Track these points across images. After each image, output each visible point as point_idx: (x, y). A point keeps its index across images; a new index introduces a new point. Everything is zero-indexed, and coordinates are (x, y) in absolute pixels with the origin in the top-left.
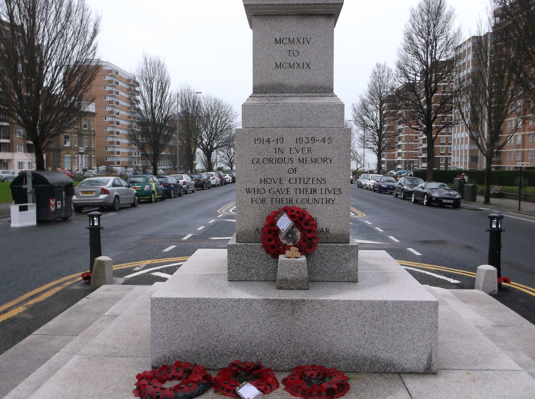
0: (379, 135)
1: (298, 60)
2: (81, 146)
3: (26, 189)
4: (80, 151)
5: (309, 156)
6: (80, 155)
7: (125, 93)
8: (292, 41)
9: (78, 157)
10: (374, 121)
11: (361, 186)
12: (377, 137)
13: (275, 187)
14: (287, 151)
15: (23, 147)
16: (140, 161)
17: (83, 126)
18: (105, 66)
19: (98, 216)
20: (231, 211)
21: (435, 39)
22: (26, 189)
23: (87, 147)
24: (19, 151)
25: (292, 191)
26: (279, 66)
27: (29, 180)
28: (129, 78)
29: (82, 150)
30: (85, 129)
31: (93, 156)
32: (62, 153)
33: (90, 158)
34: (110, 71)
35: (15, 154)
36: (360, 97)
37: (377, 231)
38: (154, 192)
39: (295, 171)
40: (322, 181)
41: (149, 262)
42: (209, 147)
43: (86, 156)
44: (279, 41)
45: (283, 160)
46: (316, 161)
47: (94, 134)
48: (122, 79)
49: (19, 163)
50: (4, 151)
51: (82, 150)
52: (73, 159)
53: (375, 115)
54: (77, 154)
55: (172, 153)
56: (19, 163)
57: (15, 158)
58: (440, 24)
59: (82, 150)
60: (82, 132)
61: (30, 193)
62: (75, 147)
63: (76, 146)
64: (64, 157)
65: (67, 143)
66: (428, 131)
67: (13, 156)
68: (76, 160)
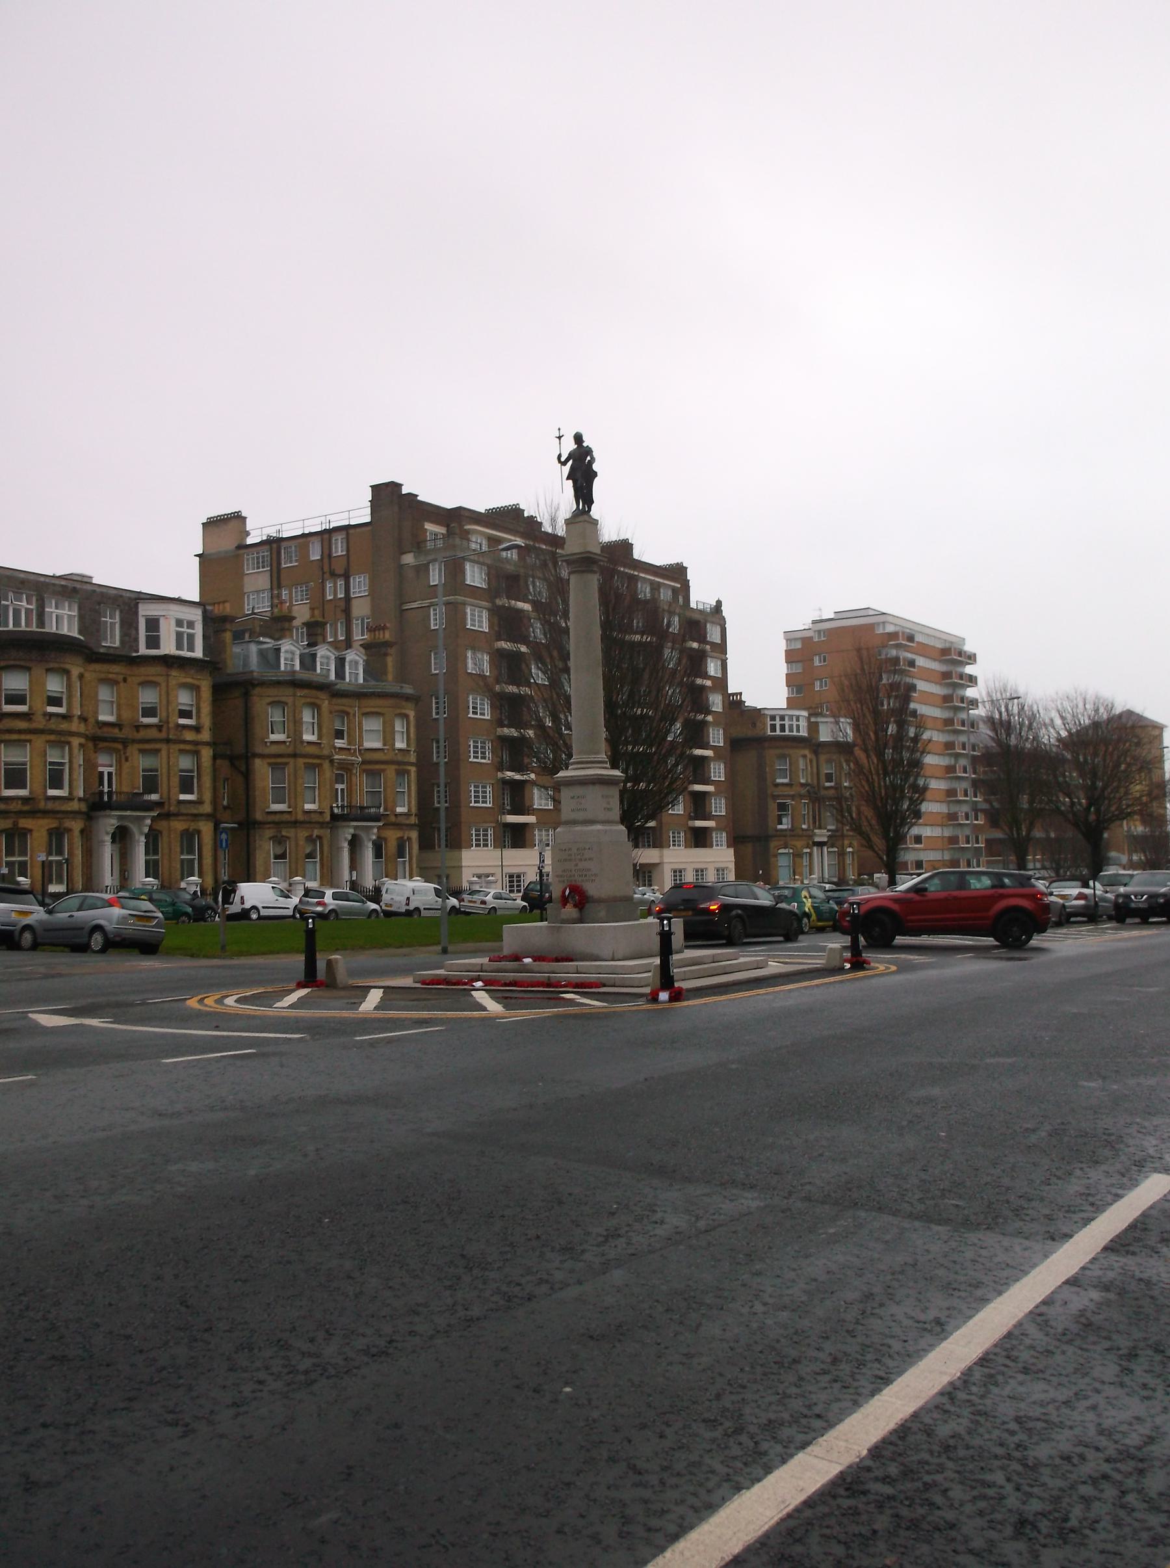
2: (820, 828)
4: (817, 839)
6: (815, 848)
7: (936, 683)
9: (811, 854)
15: (682, 834)
16: (983, 859)
17: (823, 778)
18: (878, 624)
23: (833, 827)
24: (674, 845)
28: (947, 645)
29: (821, 835)
30: (827, 784)
31: (850, 850)
32: (773, 844)
33: (842, 854)
34: (894, 636)
35: (666, 851)
38: (808, 915)
40: (589, 870)
42: (1092, 817)
43: (830, 850)
44: (573, 798)
47: (851, 794)
48: (925, 650)
49: (675, 871)
50: (644, 846)
51: (821, 835)
52: (797, 860)
54: (807, 847)
55: (1047, 832)
56: (675, 871)
57: (665, 861)
59: (821, 836)
60: (823, 792)
62: (803, 830)
63: (804, 827)
64: (776, 856)
65: (784, 820)
67: (661, 857)
68: (805, 861)
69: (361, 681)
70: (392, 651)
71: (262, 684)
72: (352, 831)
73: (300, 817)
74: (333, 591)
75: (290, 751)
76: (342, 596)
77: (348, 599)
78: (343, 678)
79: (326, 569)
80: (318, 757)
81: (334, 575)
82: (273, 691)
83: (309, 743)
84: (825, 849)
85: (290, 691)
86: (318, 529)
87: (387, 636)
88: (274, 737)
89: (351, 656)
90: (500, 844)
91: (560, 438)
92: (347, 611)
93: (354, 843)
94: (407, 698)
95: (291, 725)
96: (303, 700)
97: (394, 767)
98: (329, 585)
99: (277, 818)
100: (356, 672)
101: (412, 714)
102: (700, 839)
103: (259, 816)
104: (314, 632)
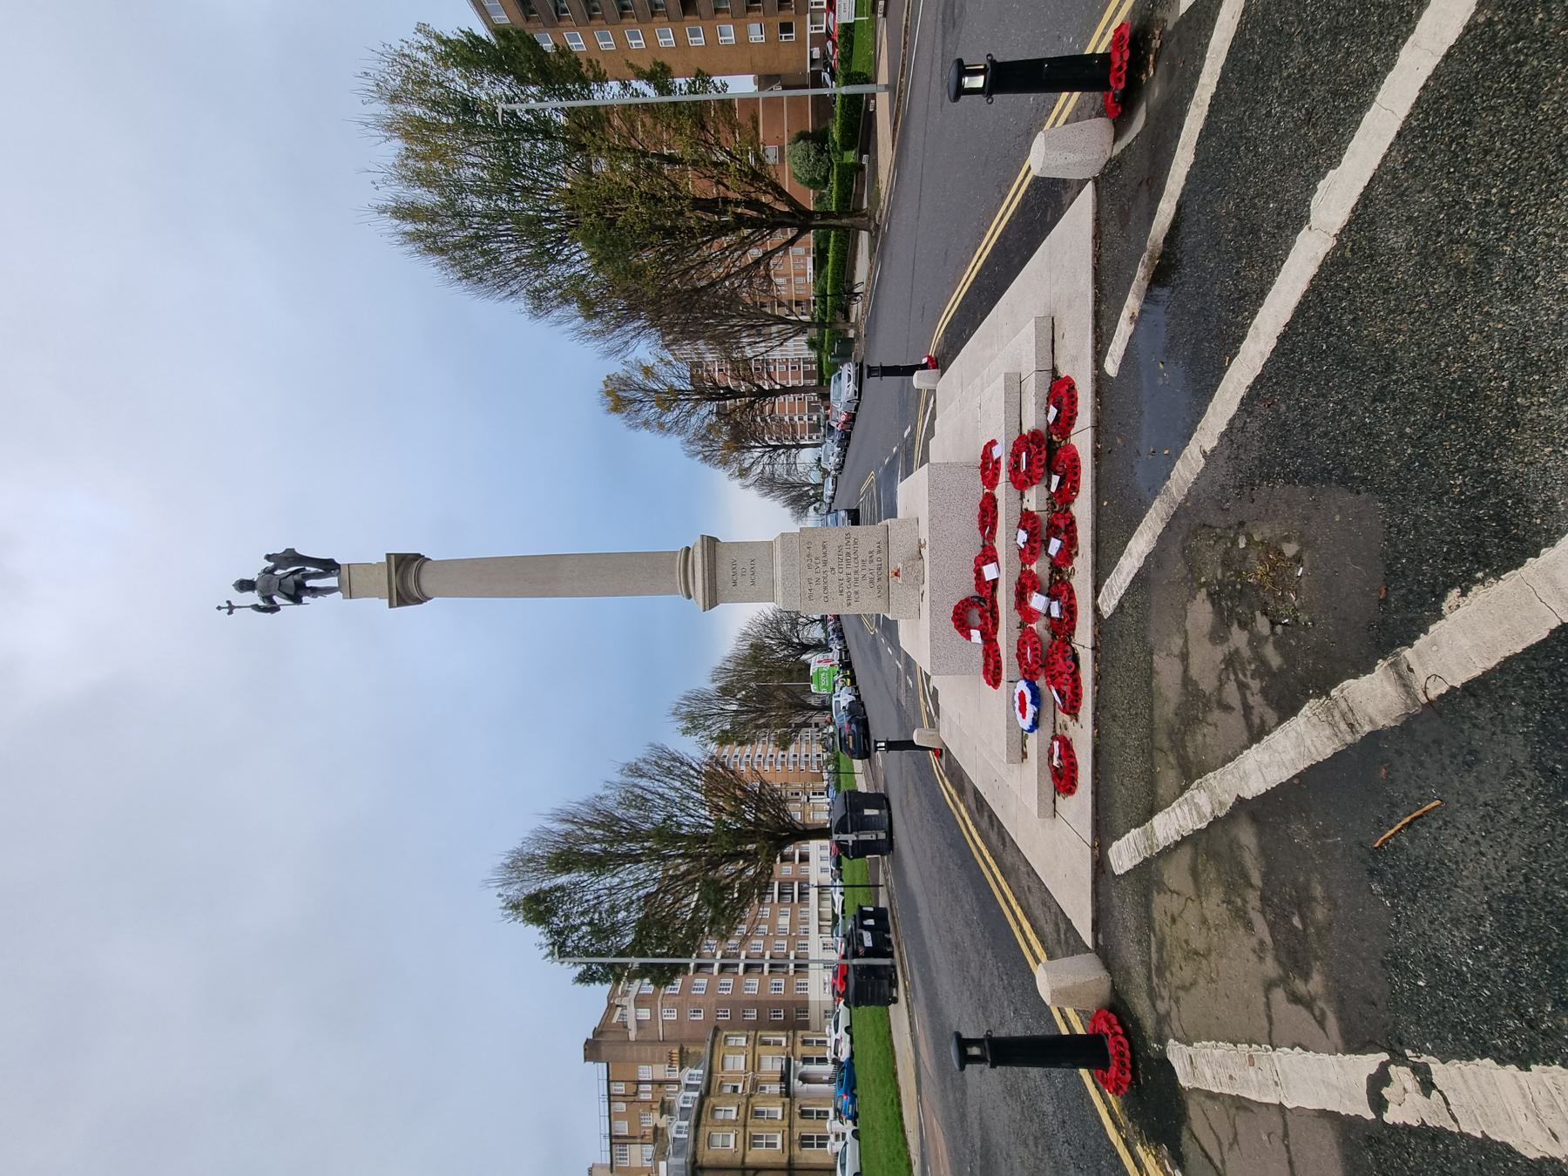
1: (748, 568)
3: (853, 841)
5: (821, 559)
8: (735, 574)
11: (840, 467)
13: (845, 584)
14: (817, 575)
19: (876, 742)
22: (853, 841)
25: (849, 571)
27: (843, 837)
37: (889, 462)
39: (833, 569)
41: (922, 699)
61: (857, 836)
66: (773, 393)
69: (701, 1072)
70: (686, 1047)
71: (695, 1154)
72: (796, 1080)
73: (786, 1122)
74: (646, 1093)
75: (741, 1130)
76: (650, 1086)
77: (652, 1082)
78: (698, 1085)
79: (632, 1099)
80: (747, 1107)
81: (636, 1094)
82: (700, 1145)
83: (738, 1114)
84: (811, 797)
85: (702, 1128)
86: (607, 1104)
87: (676, 1051)
88: (732, 1146)
89: (685, 1080)
90: (806, 975)
91: (231, 608)
92: (661, 1083)
93: (804, 1079)
94: (715, 1035)
95: (725, 1128)
96: (709, 1119)
97: (757, 1047)
98: (643, 1097)
99: (786, 1143)
100: (695, 1074)
101: (726, 1033)
102: (804, 858)
103: (785, 1160)
104: (665, 1108)
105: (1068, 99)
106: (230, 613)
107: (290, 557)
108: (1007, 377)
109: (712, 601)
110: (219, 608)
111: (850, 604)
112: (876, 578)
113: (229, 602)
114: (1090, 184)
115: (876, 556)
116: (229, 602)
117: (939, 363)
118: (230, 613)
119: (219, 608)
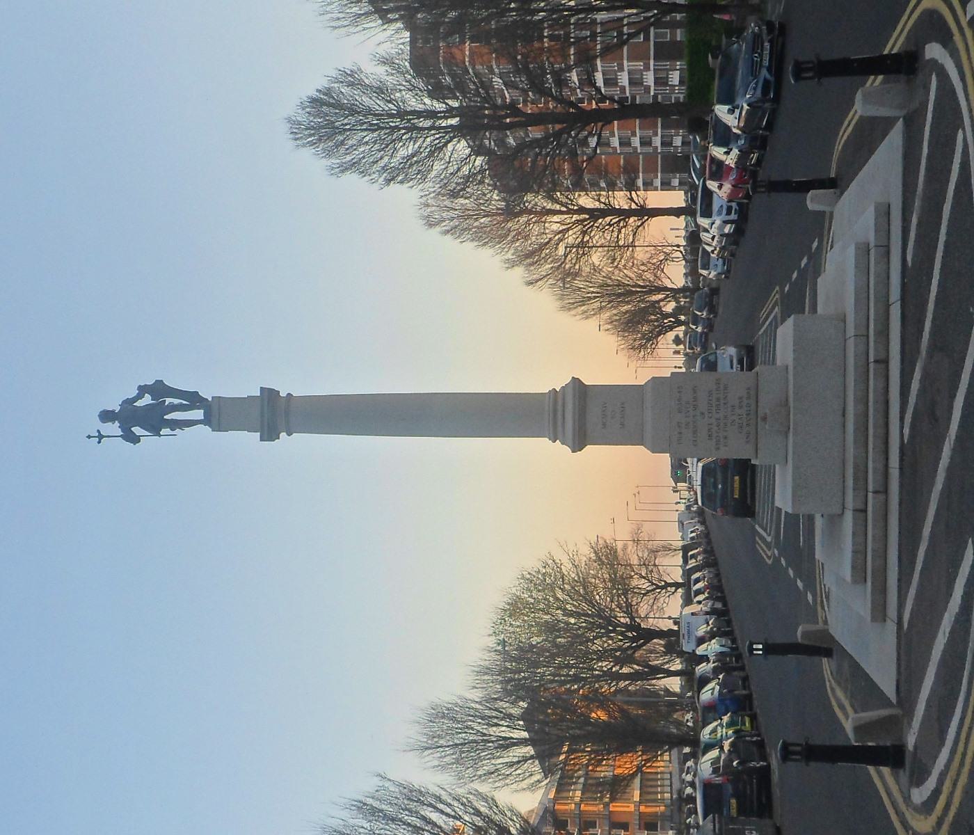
0: (603, 213)
10: (568, 230)
12: (608, 219)
20: (769, 539)
21: (402, 114)
25: (718, 416)
26: (622, 424)
36: (512, 264)
39: (702, 414)
45: (694, 422)
46: (695, 399)
53: (555, 227)
58: (378, 105)
66: (604, 117)
91: (101, 437)
105: (892, 49)
106: (99, 442)
107: (159, 390)
108: (857, 248)
109: (578, 446)
110: (89, 437)
111: (718, 449)
112: (745, 424)
113: (98, 431)
114: (901, 119)
115: (745, 401)
116: (98, 431)
117: (835, 184)
118: (99, 442)
119: (89, 437)
